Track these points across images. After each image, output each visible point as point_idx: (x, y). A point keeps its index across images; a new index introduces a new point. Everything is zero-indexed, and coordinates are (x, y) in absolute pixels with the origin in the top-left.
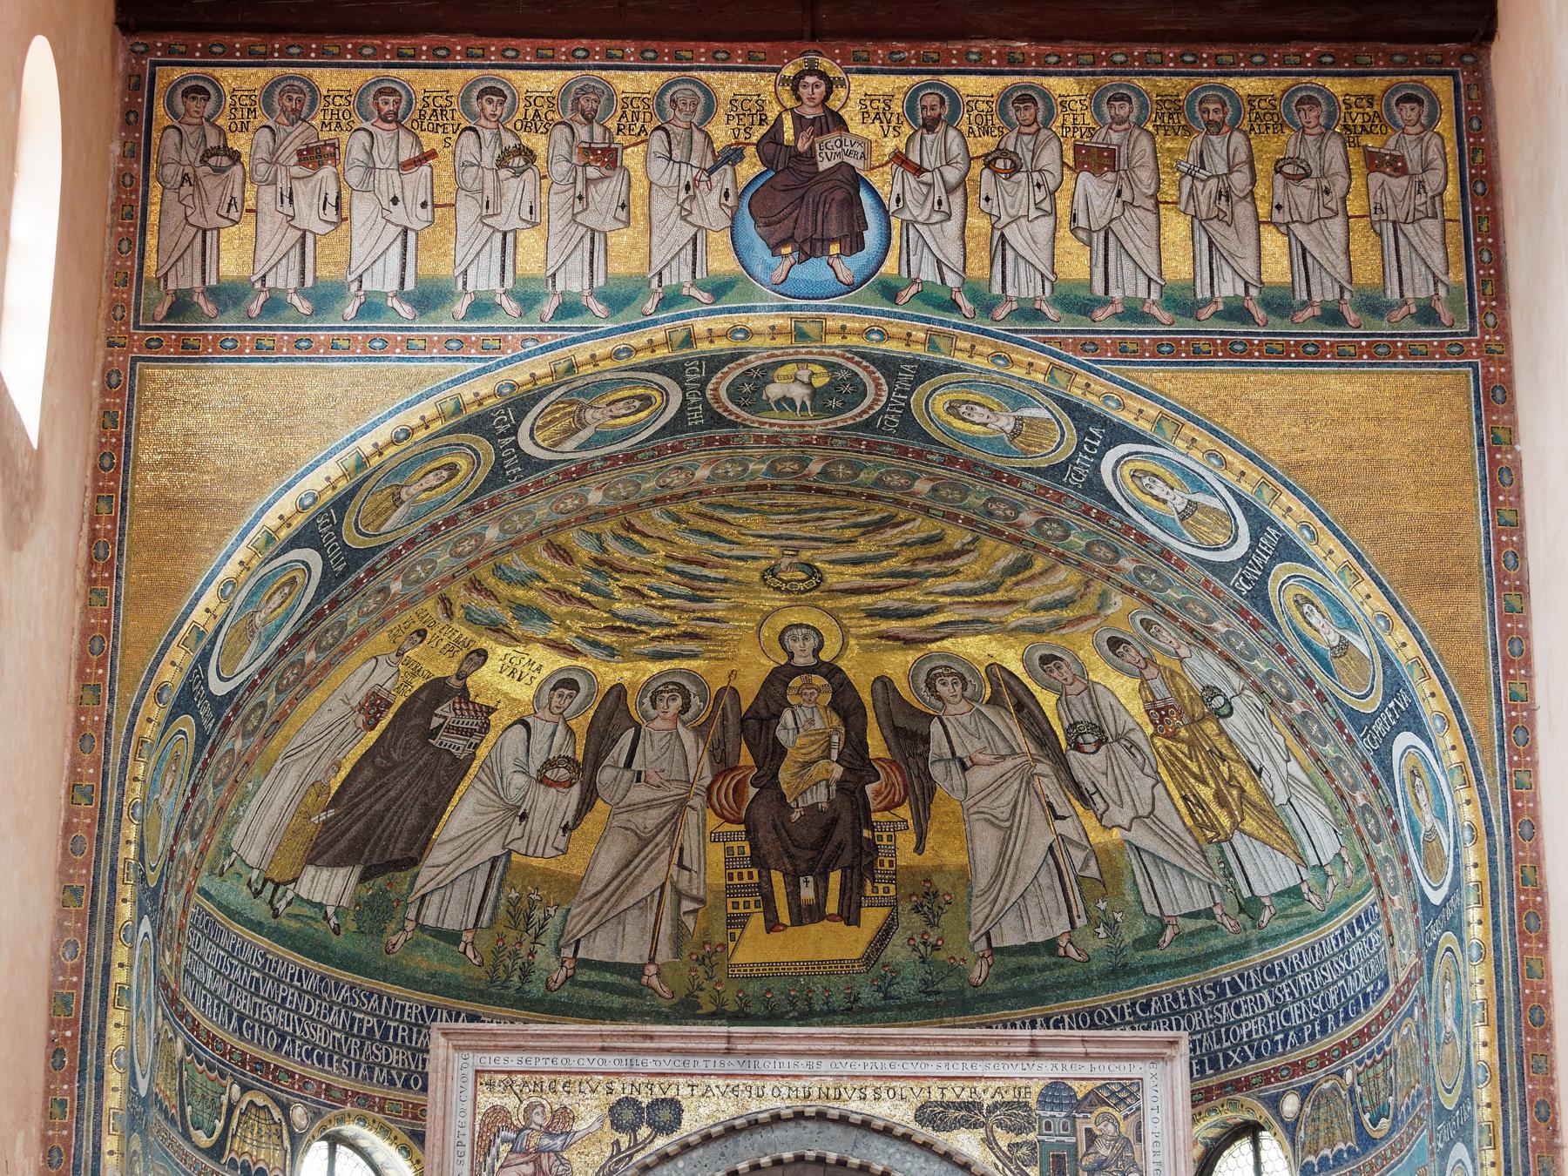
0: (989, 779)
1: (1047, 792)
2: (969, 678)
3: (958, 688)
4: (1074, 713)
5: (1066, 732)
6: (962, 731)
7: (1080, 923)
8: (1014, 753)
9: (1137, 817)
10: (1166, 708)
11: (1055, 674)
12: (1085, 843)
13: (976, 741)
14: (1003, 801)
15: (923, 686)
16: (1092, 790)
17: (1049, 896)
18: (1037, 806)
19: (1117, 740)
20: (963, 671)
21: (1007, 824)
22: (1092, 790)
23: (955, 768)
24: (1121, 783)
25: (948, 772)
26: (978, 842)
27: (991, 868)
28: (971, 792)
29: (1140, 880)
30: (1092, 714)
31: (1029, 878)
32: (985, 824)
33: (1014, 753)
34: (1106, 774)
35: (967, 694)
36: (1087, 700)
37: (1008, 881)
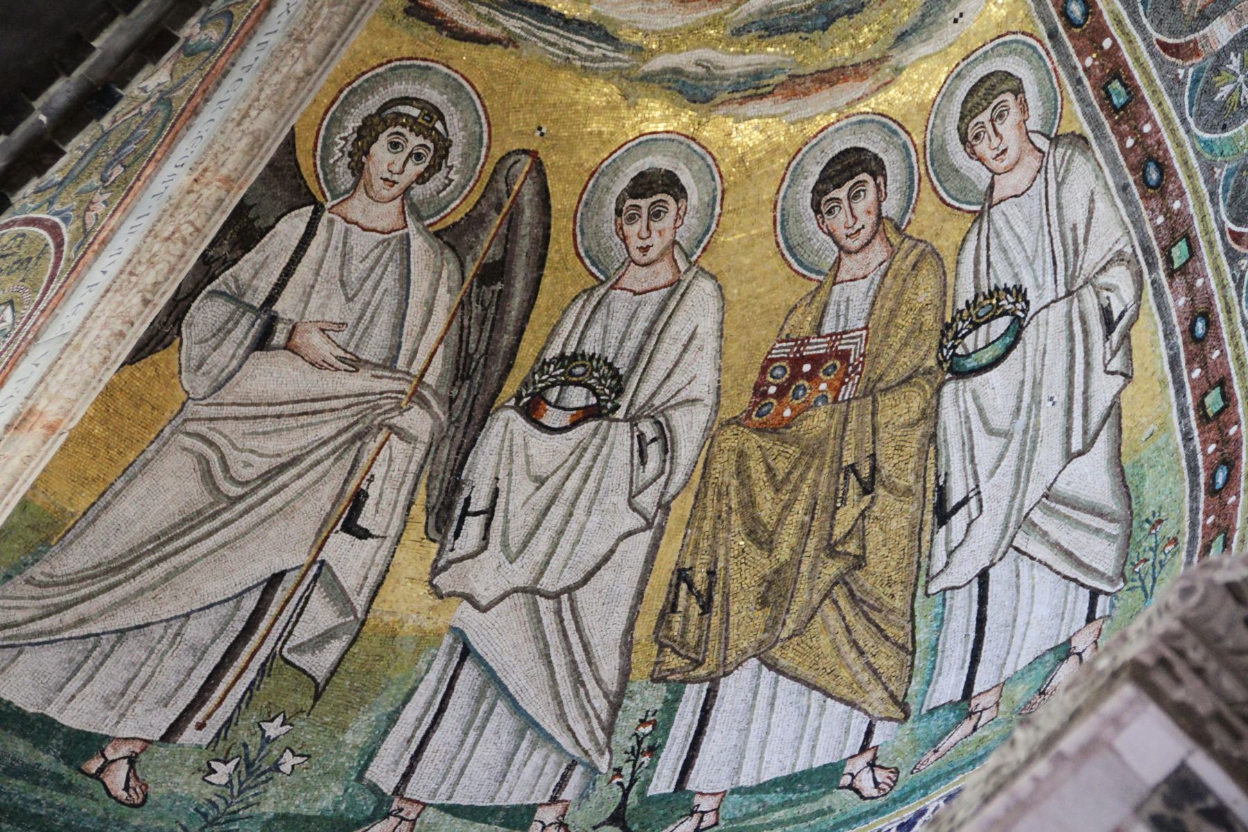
0: (287, 391)
1: (378, 471)
2: (454, 158)
3: (414, 169)
4: (595, 331)
5: (542, 365)
6: (332, 265)
7: (190, 736)
8: (389, 364)
9: (531, 591)
10: (816, 361)
11: (632, 230)
12: (360, 602)
13: (338, 299)
14: (271, 445)
15: (353, 123)
16: (480, 503)
17: (175, 663)
18: (329, 489)
19: (633, 420)
20: (458, 136)
21: (235, 491)
22: (480, 503)
23: (245, 330)
24: (557, 512)
25: (223, 331)
26: (140, 488)
27: (117, 547)
28: (226, 395)
29: (410, 713)
30: (631, 346)
31: (171, 608)
32: (189, 461)
33: (389, 364)
34: (541, 481)
35: (418, 192)
36: (647, 312)
37: (119, 592)
